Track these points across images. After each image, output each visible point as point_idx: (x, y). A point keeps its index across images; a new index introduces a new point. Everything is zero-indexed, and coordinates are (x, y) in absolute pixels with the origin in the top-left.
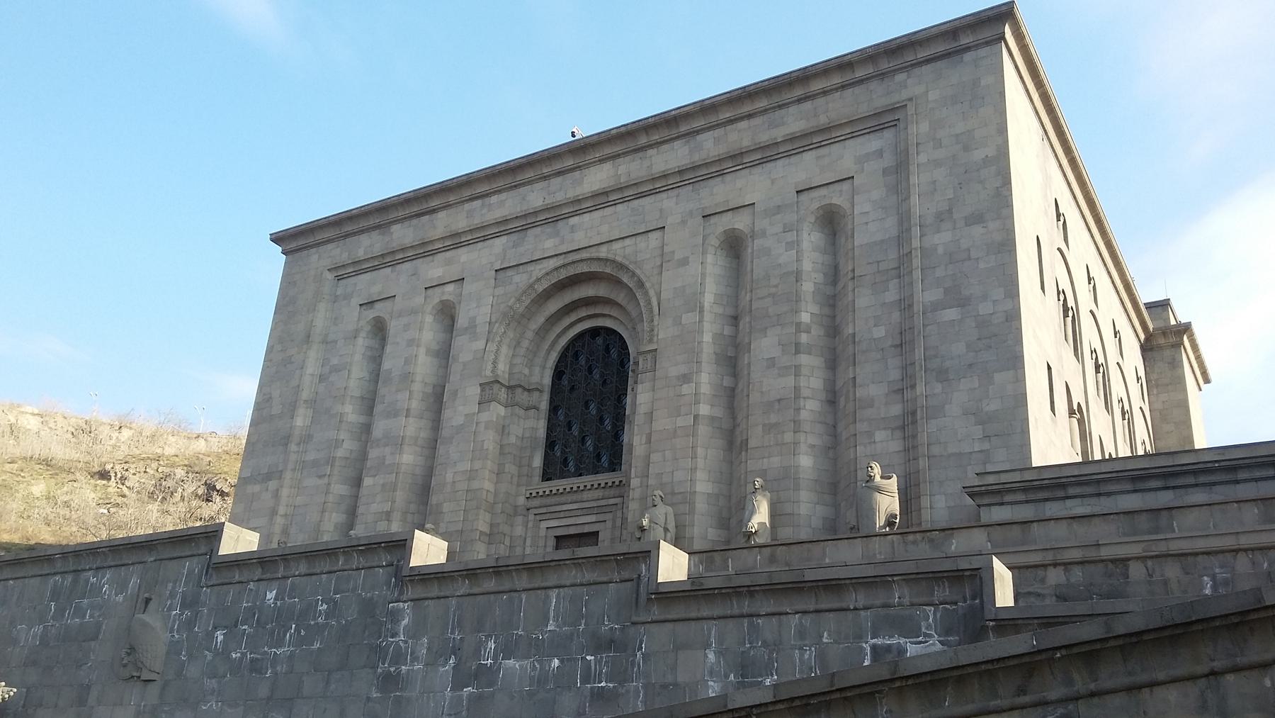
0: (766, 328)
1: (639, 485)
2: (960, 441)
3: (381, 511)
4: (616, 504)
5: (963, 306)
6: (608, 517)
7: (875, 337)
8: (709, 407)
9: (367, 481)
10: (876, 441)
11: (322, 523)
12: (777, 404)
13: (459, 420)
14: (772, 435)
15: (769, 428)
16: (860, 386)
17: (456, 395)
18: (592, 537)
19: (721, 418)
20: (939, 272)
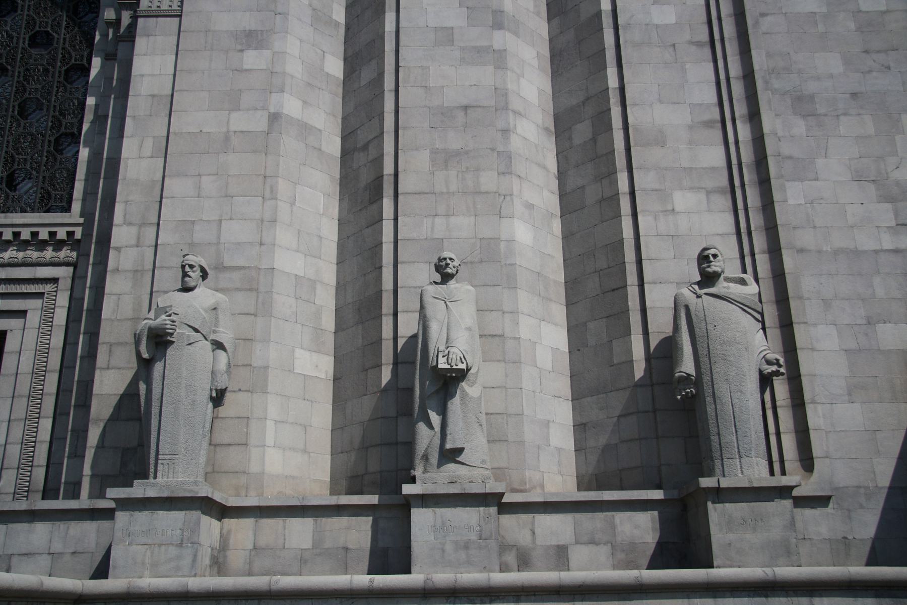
1: (133, 242)
2: (852, 227)
4: (55, 280)
7: (657, 20)
8: (300, 103)
10: (677, 209)
12: (460, 114)
14: (453, 173)
16: (635, 105)
19: (320, 130)
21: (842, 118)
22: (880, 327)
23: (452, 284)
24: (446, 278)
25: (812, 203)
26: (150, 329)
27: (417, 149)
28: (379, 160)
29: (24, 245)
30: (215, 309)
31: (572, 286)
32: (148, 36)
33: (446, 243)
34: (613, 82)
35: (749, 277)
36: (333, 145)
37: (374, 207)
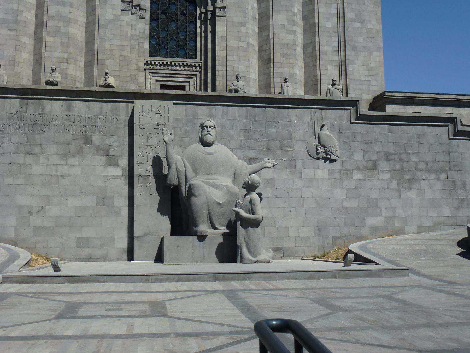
0: (280, 11)
1: (221, 69)
2: (361, 75)
3: (62, 57)
4: (196, 75)
5: (362, 23)
6: (191, 80)
9: (49, 39)
10: (328, 69)
11: (16, 57)
12: (286, 46)
13: (111, 17)
15: (283, 55)
17: (106, 2)
18: (183, 88)
20: (353, 6)
21: (362, 52)
22: (364, 95)
23: (288, 83)
24: (286, 82)
25: (354, 70)
26: (235, 89)
27: (278, 53)
28: (269, 54)
29: (188, 67)
30: (244, 85)
31: (306, 83)
32: (219, 21)
33: (284, 73)
34: (317, 40)
35: (341, 85)
36: (257, 49)
37: (269, 64)
